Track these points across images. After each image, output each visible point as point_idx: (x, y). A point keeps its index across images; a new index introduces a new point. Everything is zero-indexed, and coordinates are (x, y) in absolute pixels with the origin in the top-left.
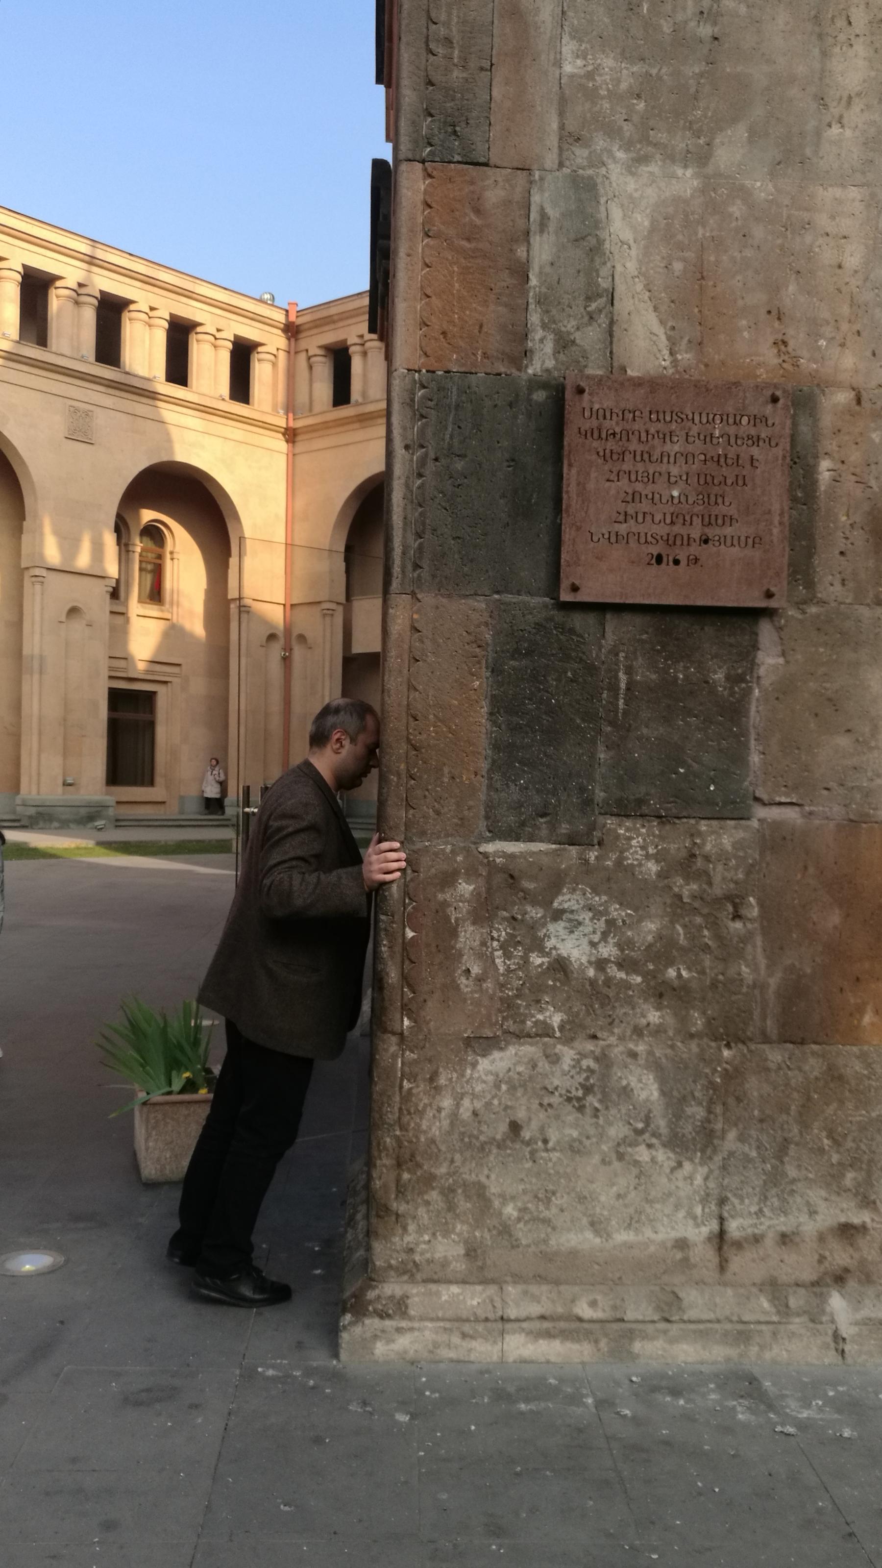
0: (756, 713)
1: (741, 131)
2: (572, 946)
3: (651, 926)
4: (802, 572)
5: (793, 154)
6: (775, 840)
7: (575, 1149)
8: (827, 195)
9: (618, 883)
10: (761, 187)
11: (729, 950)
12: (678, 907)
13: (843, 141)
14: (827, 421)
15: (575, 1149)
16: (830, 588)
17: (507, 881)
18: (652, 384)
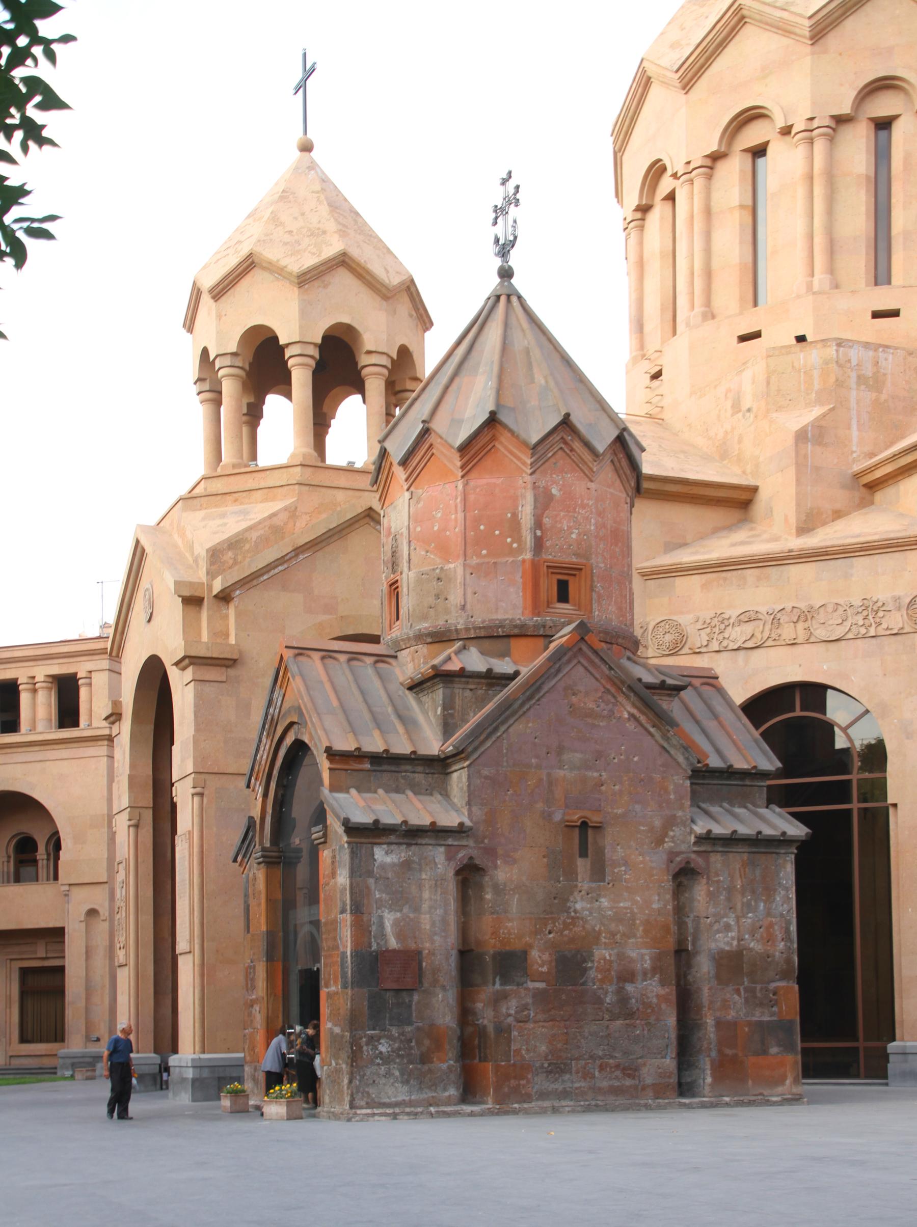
0: (414, 1007)
1: (407, 906)
2: (383, 1048)
3: (397, 1045)
4: (421, 982)
5: (417, 909)
6: (418, 1029)
7: (385, 1084)
8: (423, 916)
9: (390, 1037)
10: (412, 915)
11: (411, 1048)
12: (401, 1041)
13: (425, 906)
14: (424, 955)
15: (385, 1084)
16: (426, 985)
17: (371, 1038)
18: (394, 951)
